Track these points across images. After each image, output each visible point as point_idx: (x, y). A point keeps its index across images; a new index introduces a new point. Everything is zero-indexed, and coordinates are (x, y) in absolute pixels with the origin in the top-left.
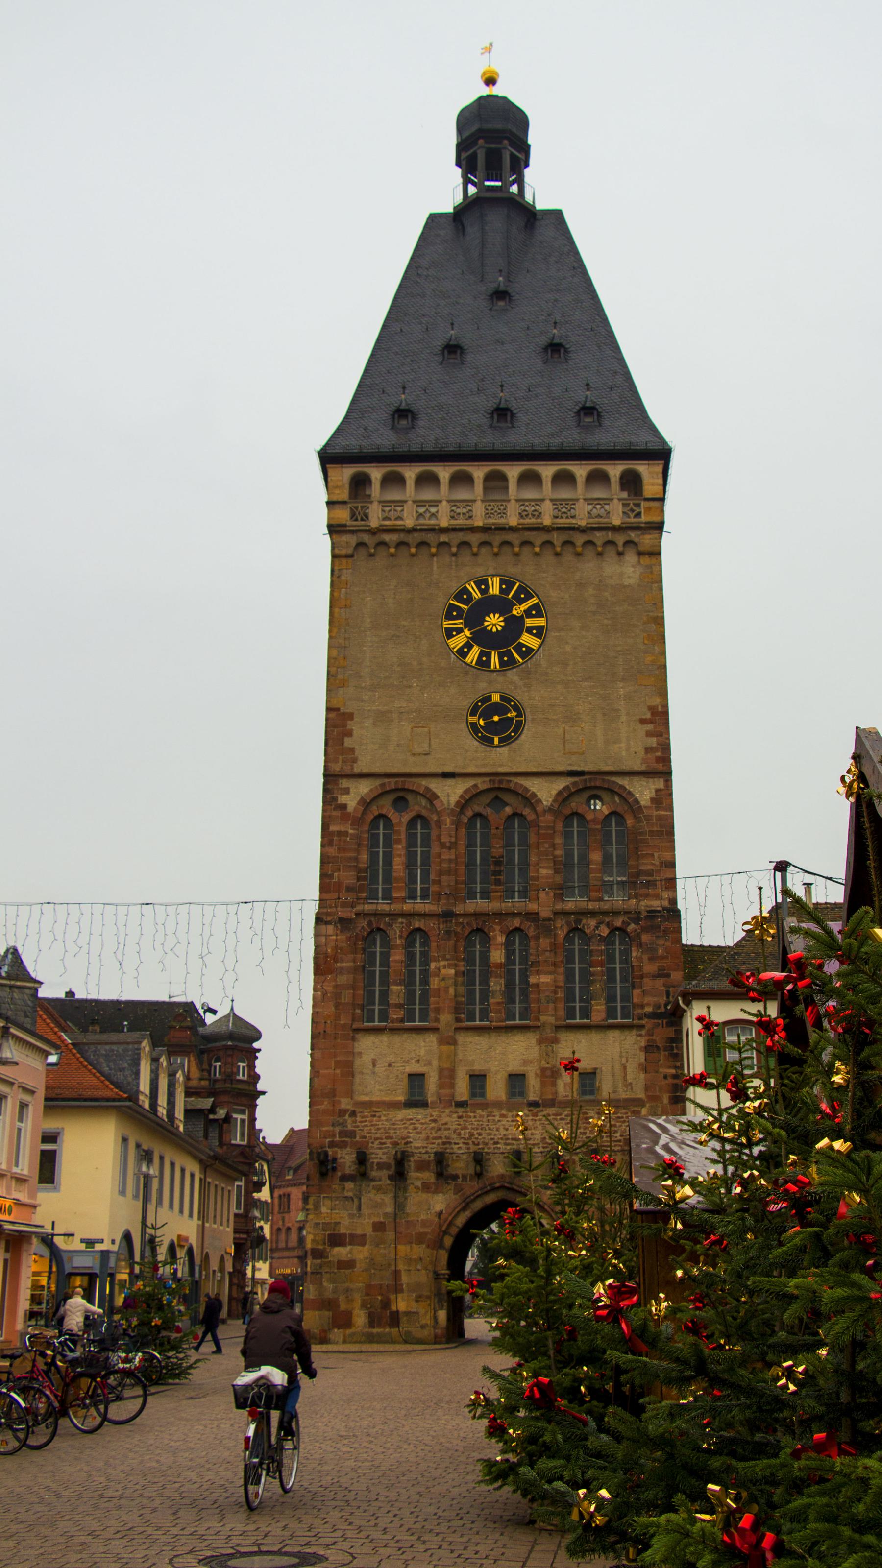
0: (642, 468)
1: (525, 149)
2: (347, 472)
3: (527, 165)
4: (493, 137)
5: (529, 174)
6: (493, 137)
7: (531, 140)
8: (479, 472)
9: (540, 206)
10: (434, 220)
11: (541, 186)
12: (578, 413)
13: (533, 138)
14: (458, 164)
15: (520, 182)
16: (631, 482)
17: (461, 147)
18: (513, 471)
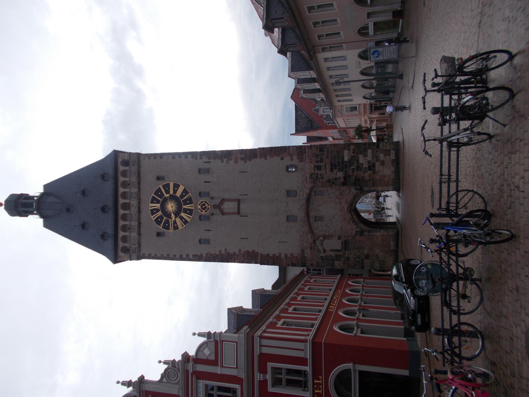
0: (120, 160)
1: (22, 195)
2: (121, 254)
3: (28, 195)
4: (19, 205)
5: (31, 194)
6: (19, 205)
7: (19, 193)
8: (121, 212)
9: (42, 191)
10: (46, 225)
11: (35, 190)
12: (104, 180)
13: (19, 192)
14: (27, 216)
15: (33, 197)
16: (126, 163)
17: (21, 215)
18: (121, 201)
